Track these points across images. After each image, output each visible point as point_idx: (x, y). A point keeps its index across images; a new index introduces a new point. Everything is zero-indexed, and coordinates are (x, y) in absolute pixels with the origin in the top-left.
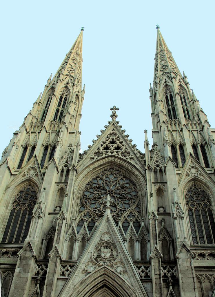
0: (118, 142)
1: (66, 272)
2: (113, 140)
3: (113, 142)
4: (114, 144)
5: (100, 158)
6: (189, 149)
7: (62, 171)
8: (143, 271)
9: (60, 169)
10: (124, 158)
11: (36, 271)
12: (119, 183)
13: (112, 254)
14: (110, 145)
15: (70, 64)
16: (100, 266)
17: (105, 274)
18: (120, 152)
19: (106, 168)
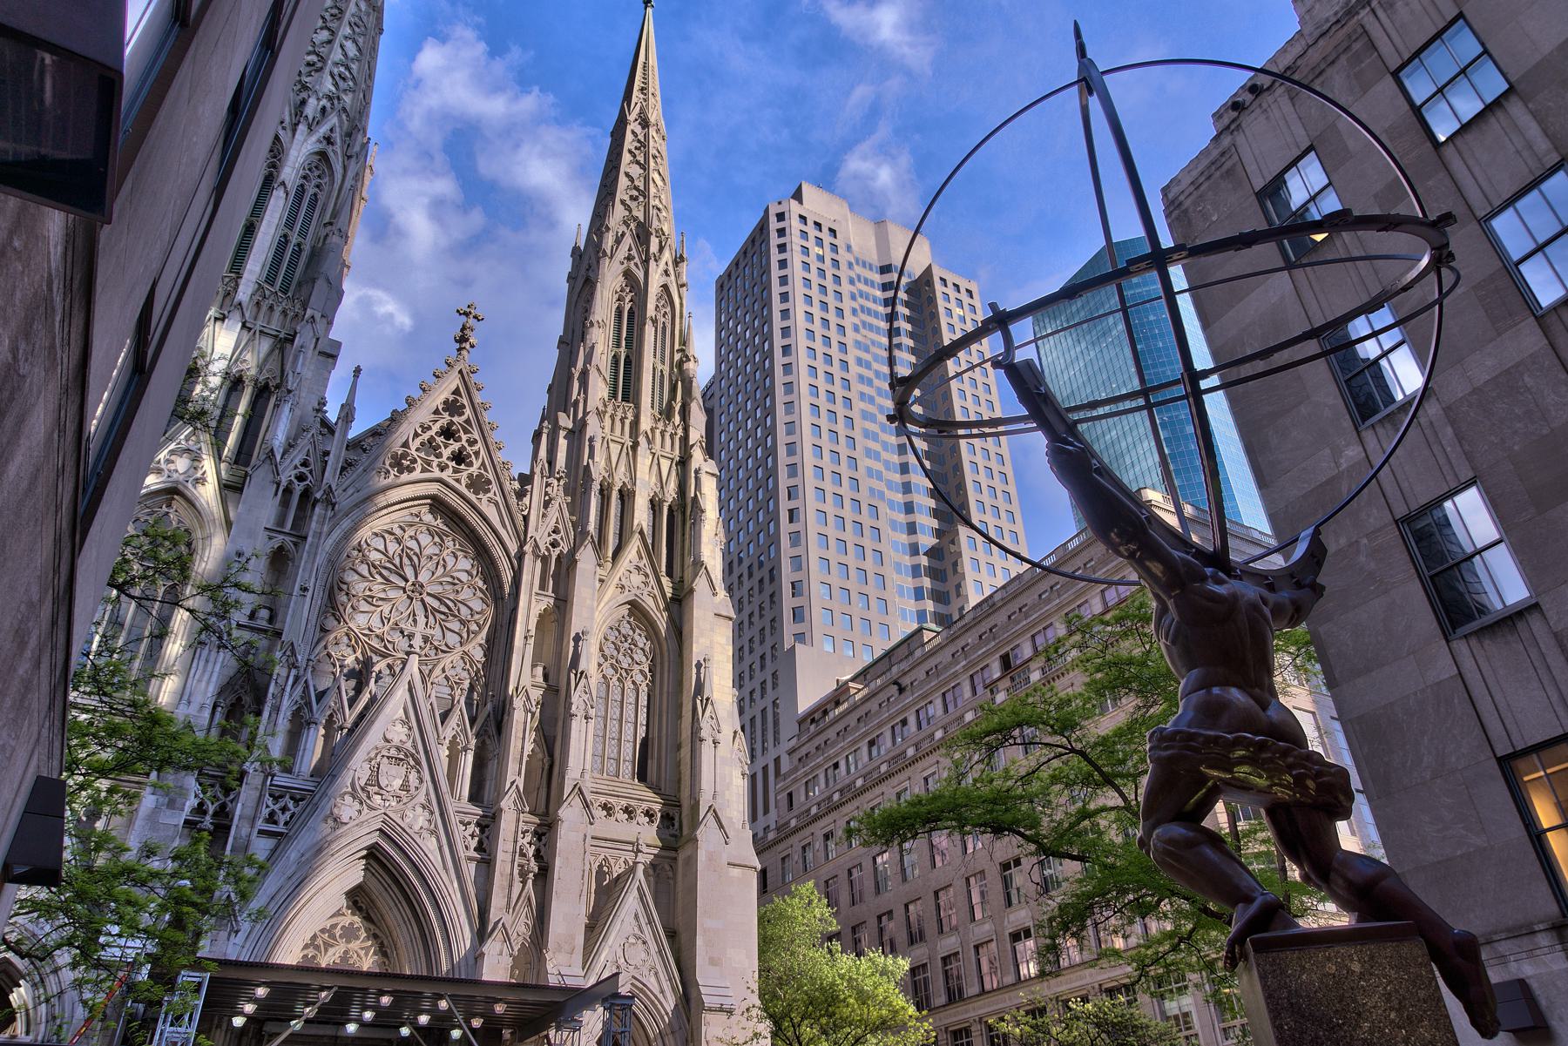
0: (464, 437)
1: (280, 813)
2: (451, 423)
3: (448, 433)
4: (451, 441)
5: (405, 477)
6: (641, 515)
7: (288, 491)
8: (472, 836)
9: (284, 483)
10: (472, 497)
11: (195, 802)
12: (445, 567)
13: (406, 780)
14: (441, 440)
15: (342, 47)
16: (371, 808)
17: (380, 830)
18: (465, 474)
19: (414, 510)
